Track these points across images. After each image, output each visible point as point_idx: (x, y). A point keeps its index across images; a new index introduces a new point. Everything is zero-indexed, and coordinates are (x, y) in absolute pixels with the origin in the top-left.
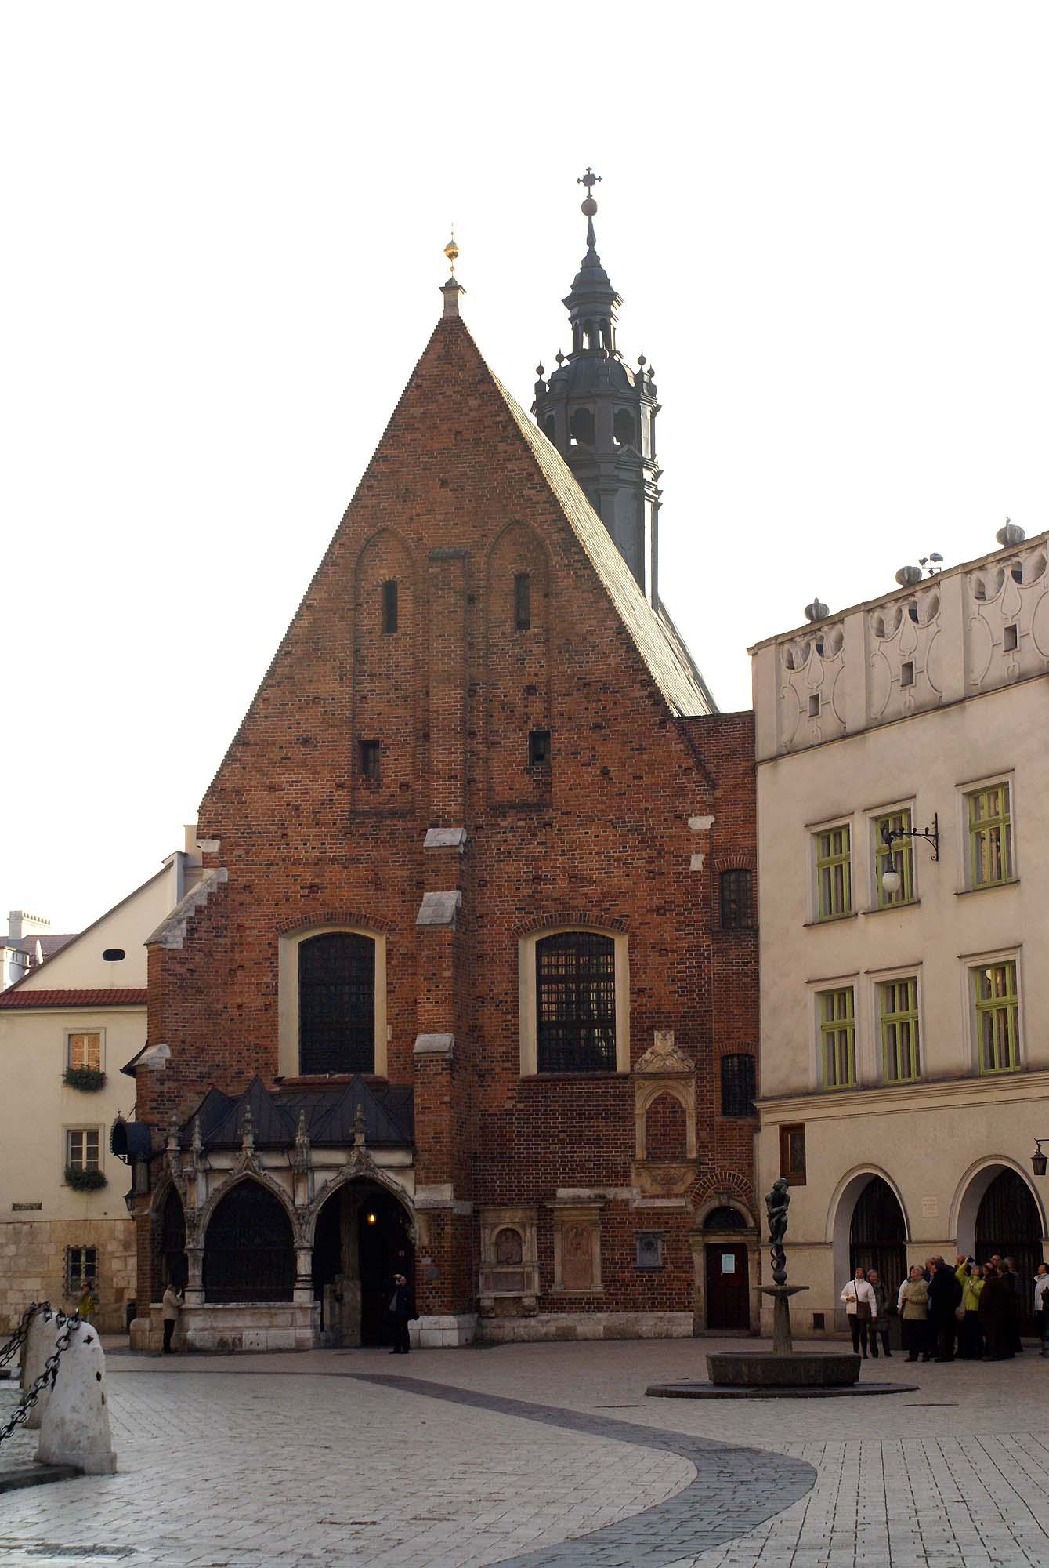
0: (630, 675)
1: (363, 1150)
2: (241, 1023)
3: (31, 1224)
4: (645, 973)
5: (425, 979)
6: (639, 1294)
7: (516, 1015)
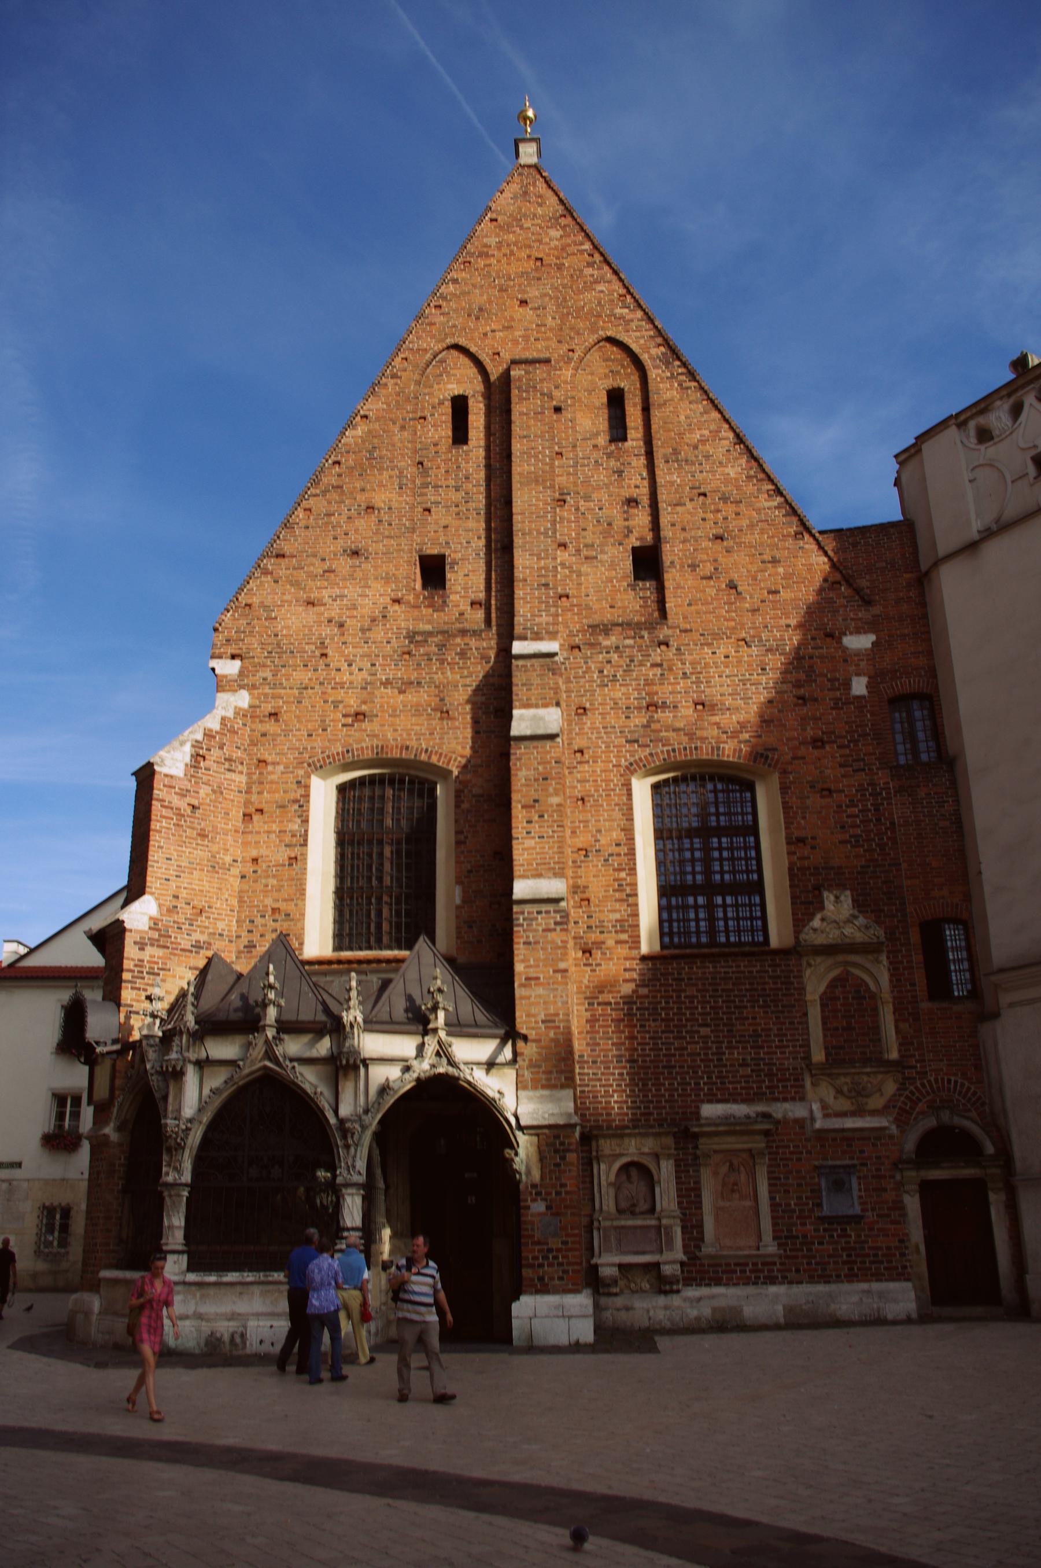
0: (754, 485)
1: (442, 1034)
3: (9, 1182)
4: (804, 818)
5: (523, 807)
6: (829, 1256)
7: (633, 870)
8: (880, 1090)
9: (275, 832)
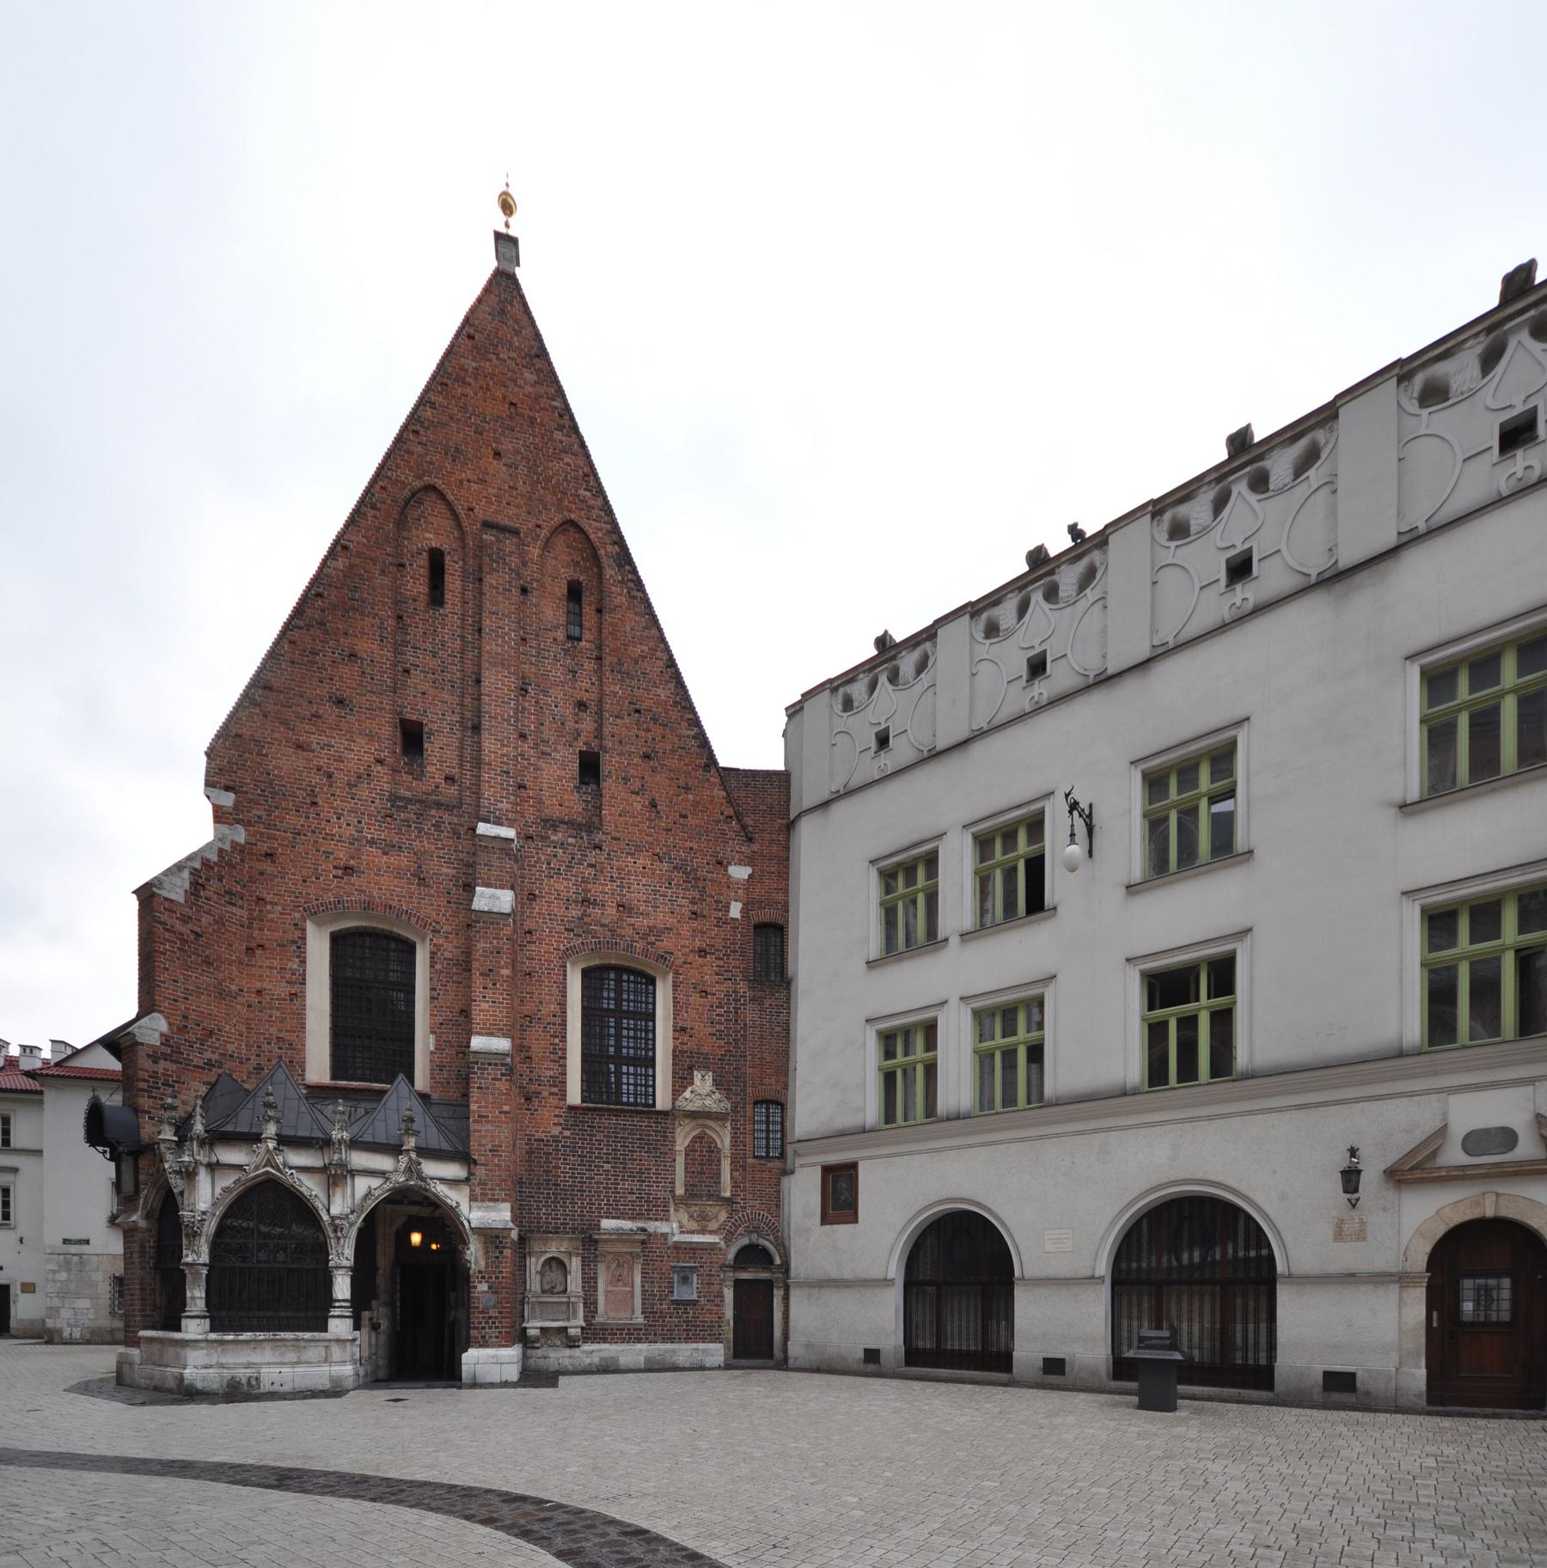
2: (260, 1011)
8: (716, 1217)
9: (276, 968)
